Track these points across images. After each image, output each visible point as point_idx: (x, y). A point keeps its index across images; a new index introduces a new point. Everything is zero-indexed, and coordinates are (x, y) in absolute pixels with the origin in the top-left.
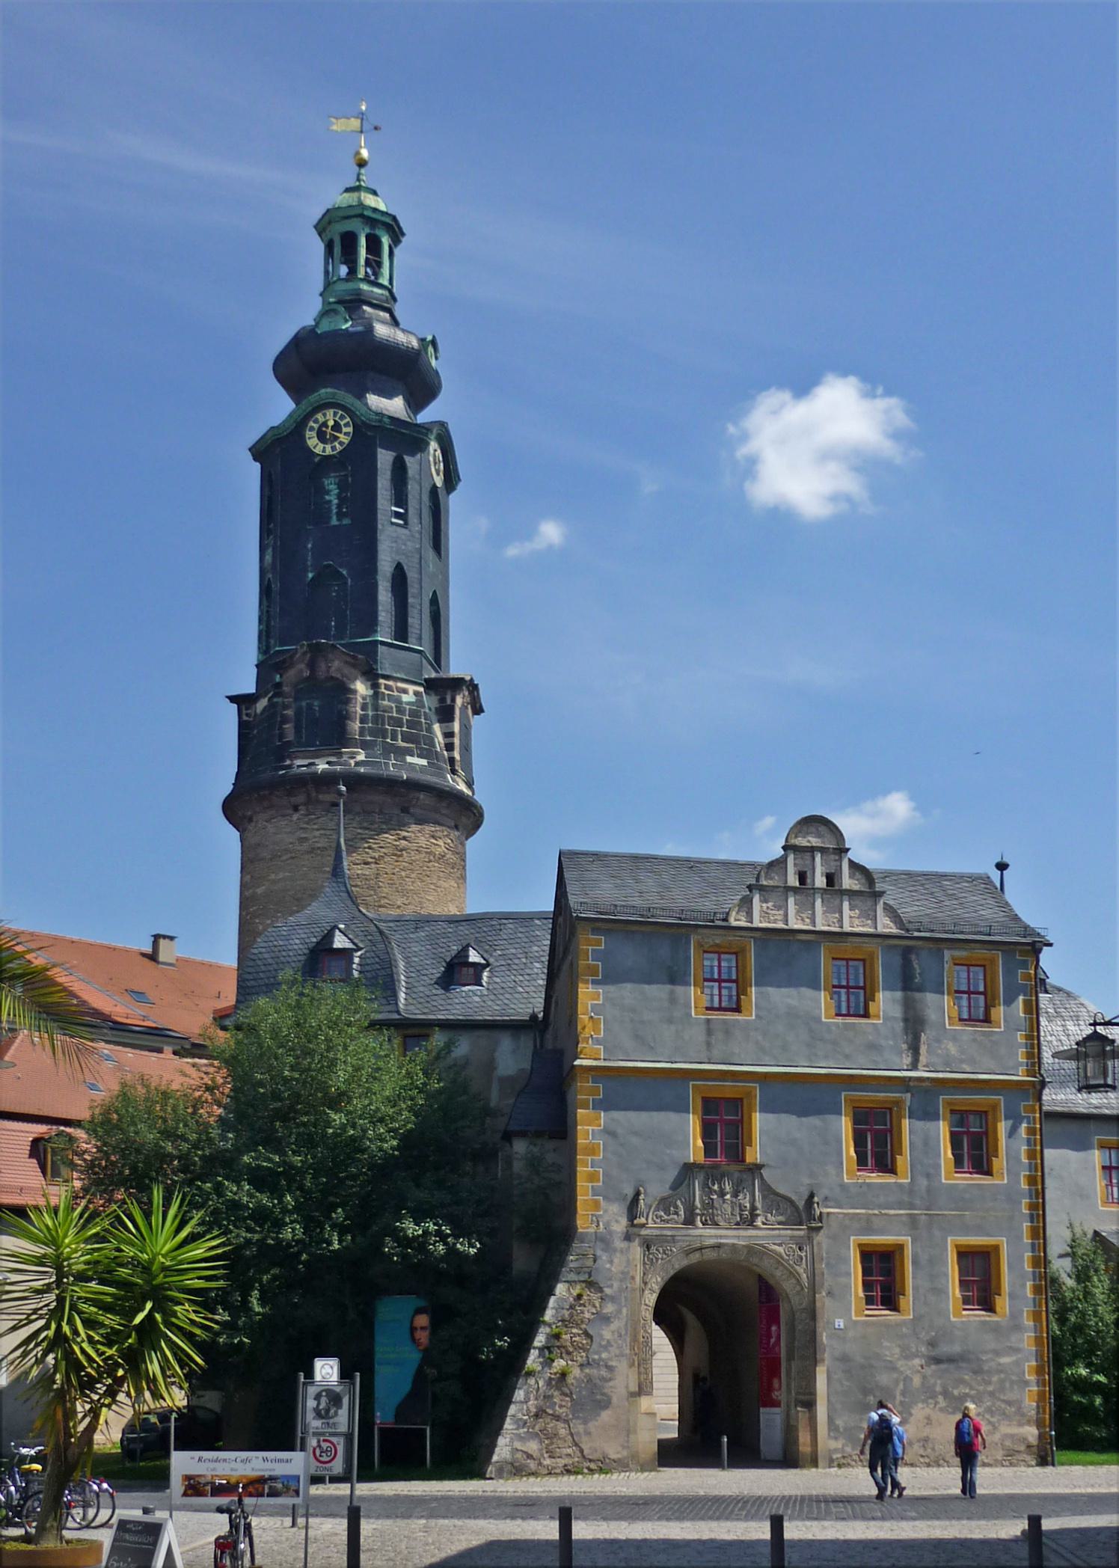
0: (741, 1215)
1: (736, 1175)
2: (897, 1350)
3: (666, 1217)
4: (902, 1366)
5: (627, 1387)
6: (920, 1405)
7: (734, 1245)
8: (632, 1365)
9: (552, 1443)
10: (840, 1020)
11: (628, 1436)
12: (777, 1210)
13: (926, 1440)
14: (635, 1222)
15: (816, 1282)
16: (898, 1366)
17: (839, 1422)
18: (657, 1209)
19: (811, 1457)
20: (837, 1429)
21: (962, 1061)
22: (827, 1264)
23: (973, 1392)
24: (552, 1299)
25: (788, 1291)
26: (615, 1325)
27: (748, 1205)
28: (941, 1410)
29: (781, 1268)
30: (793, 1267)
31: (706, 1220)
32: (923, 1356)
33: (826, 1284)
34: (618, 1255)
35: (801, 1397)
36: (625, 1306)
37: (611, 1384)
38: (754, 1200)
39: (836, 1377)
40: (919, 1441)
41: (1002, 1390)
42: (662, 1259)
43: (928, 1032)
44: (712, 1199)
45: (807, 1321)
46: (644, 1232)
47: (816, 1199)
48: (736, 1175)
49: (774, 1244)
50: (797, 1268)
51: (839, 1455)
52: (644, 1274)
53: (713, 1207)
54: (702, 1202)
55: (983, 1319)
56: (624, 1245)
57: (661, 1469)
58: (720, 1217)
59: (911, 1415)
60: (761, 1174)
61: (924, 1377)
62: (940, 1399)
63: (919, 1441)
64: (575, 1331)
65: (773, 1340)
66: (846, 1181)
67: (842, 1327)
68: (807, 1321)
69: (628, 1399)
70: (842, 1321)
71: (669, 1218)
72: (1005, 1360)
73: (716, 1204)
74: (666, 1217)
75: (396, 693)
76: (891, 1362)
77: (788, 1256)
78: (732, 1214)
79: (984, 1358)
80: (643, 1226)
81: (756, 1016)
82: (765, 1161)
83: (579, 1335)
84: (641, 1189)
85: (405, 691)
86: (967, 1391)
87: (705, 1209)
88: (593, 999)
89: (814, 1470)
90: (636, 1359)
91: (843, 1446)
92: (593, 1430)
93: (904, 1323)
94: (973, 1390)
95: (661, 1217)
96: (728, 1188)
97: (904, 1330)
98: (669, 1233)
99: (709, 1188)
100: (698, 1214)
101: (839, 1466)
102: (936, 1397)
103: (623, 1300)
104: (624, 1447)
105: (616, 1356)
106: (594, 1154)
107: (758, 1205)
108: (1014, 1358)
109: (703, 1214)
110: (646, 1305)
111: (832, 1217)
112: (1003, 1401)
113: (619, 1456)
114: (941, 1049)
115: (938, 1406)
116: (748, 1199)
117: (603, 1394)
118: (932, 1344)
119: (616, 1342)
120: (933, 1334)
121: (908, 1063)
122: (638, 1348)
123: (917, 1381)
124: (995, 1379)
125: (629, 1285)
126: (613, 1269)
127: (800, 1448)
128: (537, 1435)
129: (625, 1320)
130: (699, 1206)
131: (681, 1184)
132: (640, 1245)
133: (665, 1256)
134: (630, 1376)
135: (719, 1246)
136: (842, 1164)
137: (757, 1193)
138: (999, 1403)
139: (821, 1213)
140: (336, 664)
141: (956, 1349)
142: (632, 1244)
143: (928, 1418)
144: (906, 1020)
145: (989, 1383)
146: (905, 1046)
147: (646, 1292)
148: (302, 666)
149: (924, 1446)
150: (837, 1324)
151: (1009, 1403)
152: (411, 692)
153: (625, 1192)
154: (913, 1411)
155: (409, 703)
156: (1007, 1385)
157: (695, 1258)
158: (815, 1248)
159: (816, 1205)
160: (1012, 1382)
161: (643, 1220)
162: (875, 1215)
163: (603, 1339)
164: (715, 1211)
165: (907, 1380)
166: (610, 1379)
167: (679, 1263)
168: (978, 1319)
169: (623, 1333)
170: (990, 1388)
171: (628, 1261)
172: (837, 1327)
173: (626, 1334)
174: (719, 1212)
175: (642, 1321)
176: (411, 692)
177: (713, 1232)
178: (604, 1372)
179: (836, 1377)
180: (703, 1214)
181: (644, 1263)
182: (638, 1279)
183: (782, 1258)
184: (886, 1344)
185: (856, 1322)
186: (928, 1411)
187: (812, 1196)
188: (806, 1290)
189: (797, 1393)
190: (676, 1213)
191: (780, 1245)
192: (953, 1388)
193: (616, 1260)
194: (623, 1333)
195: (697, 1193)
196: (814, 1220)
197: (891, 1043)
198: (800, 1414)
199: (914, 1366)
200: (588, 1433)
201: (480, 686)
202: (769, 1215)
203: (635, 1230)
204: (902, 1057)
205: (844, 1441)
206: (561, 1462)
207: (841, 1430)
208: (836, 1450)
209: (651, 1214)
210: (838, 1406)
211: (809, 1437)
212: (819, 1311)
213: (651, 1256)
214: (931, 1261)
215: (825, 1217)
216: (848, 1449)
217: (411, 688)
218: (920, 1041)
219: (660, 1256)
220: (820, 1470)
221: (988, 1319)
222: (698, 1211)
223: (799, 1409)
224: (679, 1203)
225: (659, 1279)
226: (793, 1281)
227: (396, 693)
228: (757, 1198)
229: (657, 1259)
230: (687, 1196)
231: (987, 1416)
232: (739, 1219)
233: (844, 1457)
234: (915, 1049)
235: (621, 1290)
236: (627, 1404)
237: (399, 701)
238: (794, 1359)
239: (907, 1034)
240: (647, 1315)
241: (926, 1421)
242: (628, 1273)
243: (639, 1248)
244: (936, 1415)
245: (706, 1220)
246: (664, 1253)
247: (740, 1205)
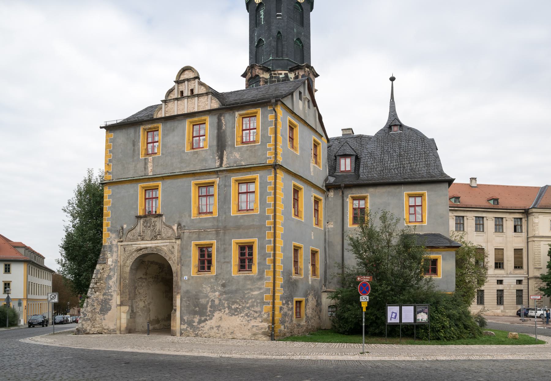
2: (209, 289)
4: (210, 295)
5: (117, 303)
6: (218, 312)
8: (118, 295)
9: (94, 323)
10: (192, 151)
13: (219, 327)
15: (345, 257)
16: (209, 295)
17: (185, 318)
21: (241, 161)
23: (240, 307)
24: (95, 270)
26: (114, 279)
28: (226, 314)
32: (219, 291)
37: (111, 301)
39: (184, 299)
40: (216, 327)
41: (253, 306)
43: (227, 150)
55: (246, 275)
59: (214, 316)
61: (220, 300)
62: (227, 309)
63: (216, 327)
64: (101, 282)
67: (187, 279)
69: (117, 307)
70: (187, 277)
72: (256, 293)
75: (278, 75)
76: (206, 293)
79: (246, 292)
81: (162, 154)
83: (103, 283)
85: (281, 74)
86: (238, 306)
88: (109, 158)
91: (187, 328)
92: (106, 318)
93: (212, 277)
94: (241, 306)
97: (212, 280)
102: (225, 308)
104: (115, 325)
106: (108, 216)
108: (259, 292)
111: (186, 233)
112: (253, 311)
114: (232, 156)
115: (225, 312)
117: (110, 305)
118: (224, 286)
120: (224, 282)
121: (218, 165)
123: (217, 302)
124: (250, 301)
128: (90, 319)
135: (146, 248)
136: (191, 211)
138: (251, 312)
140: (257, 70)
141: (234, 288)
143: (221, 318)
144: (218, 146)
145: (247, 303)
146: (217, 158)
148: (249, 74)
149: (218, 329)
150: (185, 278)
151: (256, 312)
152: (283, 74)
154: (215, 314)
155: (282, 78)
156: (255, 304)
157: (141, 253)
160: (257, 303)
162: (203, 232)
163: (109, 285)
165: (213, 301)
166: (111, 300)
167: (136, 255)
168: (244, 275)
169: (115, 282)
170: (248, 305)
176: (283, 74)
178: (109, 297)
179: (184, 299)
184: (204, 286)
185: (193, 277)
186: (221, 314)
192: (232, 305)
197: (211, 157)
199: (215, 295)
200: (104, 319)
201: (314, 67)
204: (216, 163)
206: (97, 329)
207: (186, 321)
214: (225, 251)
216: (189, 329)
217: (283, 72)
218: (223, 154)
221: (248, 275)
227: (278, 75)
231: (246, 317)
234: (221, 158)
235: (115, 266)
237: (279, 78)
239: (218, 152)
241: (220, 319)
242: (117, 260)
244: (224, 316)
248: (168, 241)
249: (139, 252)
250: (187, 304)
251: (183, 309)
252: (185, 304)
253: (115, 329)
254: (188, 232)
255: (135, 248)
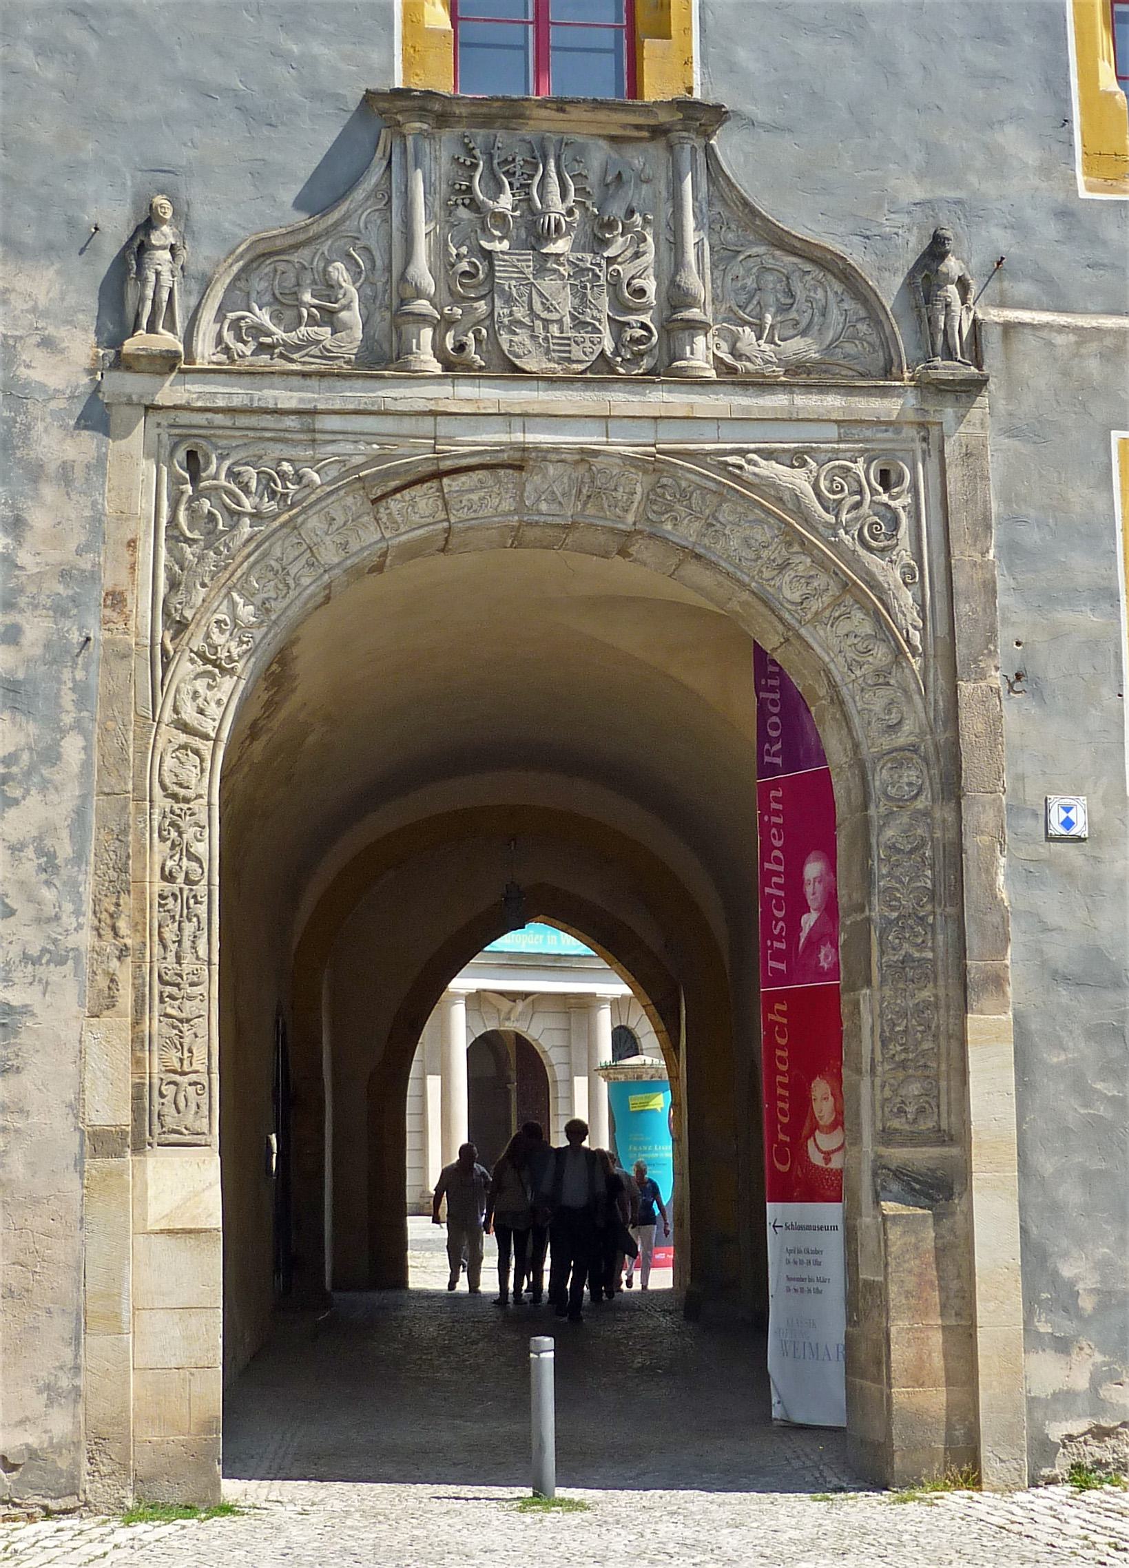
0: (619, 327)
1: (598, 156)
3: (279, 334)
5: (76, 1107)
7: (586, 455)
11: (76, 1341)
12: (783, 309)
14: (129, 346)
18: (238, 295)
19: (950, 1440)
20: (1066, 1298)
22: (1011, 550)
25: (838, 670)
27: (651, 286)
29: (803, 563)
30: (853, 560)
31: (461, 347)
33: (1005, 635)
34: (49, 492)
35: (899, 1155)
36: (78, 726)
38: (679, 264)
39: (1056, 1058)
42: (257, 516)
44: (488, 255)
45: (921, 803)
46: (171, 392)
47: (952, 266)
48: (598, 156)
49: (768, 455)
50: (874, 562)
51: (1078, 1426)
52: (174, 585)
53: (491, 289)
54: (444, 265)
56: (84, 446)
57: (231, 1489)
58: (523, 336)
60: (709, 152)
65: (809, 921)
66: (1083, 194)
67: (1080, 829)
68: (921, 803)
69: (79, 1162)
71: (292, 338)
73: (506, 278)
74: (279, 334)
77: (834, 508)
78: (579, 324)
80: (167, 363)
82: (722, 96)
84: (160, 200)
87: (458, 299)
89: (956, 1499)
90: (125, 973)
95: (258, 330)
96: (557, 206)
98: (288, 399)
99: (474, 206)
100: (422, 319)
101: (1081, 1477)
103: (68, 699)
104: (52, 1393)
105: (26, 958)
107: (697, 282)
109: (448, 323)
110: (185, 728)
111: (1030, 342)
113: (32, 1438)
116: (650, 258)
119: (31, 899)
122: (136, 927)
125: (95, 633)
126: (23, 558)
127: (899, 1394)
129: (72, 791)
130: (428, 283)
131: (353, 183)
132: (153, 453)
133: (269, 506)
134: (94, 1050)
137: (691, 235)
139: (976, 323)
142: (114, 446)
147: (185, 668)
150: (1057, 816)
153: (89, 217)
158: (954, 474)
159: (952, 291)
161: (167, 340)
164: (501, 309)
169: (65, 849)
171: (96, 522)
172: (1057, 829)
173: (79, 858)
174: (520, 313)
175: (163, 802)
177: (489, 395)
179: (1056, 1058)
180: (448, 323)
181: (175, 536)
182: (142, 605)
183: (807, 520)
187: (937, 249)
188: (916, 663)
189: (886, 1137)
190: (329, 317)
191: (796, 459)
193: (39, 519)
194: (65, 849)
195: (422, 227)
196: (949, 354)
198: (894, 1234)
202: (748, 333)
203: (132, 384)
205: (1099, 1358)
207: (1087, 1303)
208: (1064, 1400)
209: (208, 315)
210: (1071, 1194)
211: (937, 1338)
212: (973, 763)
213: (206, 505)
215: (992, 344)
219: (248, 504)
220: (986, 1503)
222: (423, 306)
223: (889, 1207)
224: (339, 272)
225: (246, 612)
226: (861, 623)
228: (691, 255)
229: (235, 516)
230: (373, 240)
232: (608, 345)
233: (1100, 1433)
236: (72, 1185)
238: (868, 982)
240: (191, 774)
242: (93, 577)
243: (148, 468)
245: (461, 347)
246: (267, 480)
247: (615, 284)
248: (833, 403)
249: (394, 504)
250: (1102, 1110)
251: (1046, 1164)
252: (1073, 1110)
253: (57, 1448)
254: (1062, 329)
255: (358, 453)
